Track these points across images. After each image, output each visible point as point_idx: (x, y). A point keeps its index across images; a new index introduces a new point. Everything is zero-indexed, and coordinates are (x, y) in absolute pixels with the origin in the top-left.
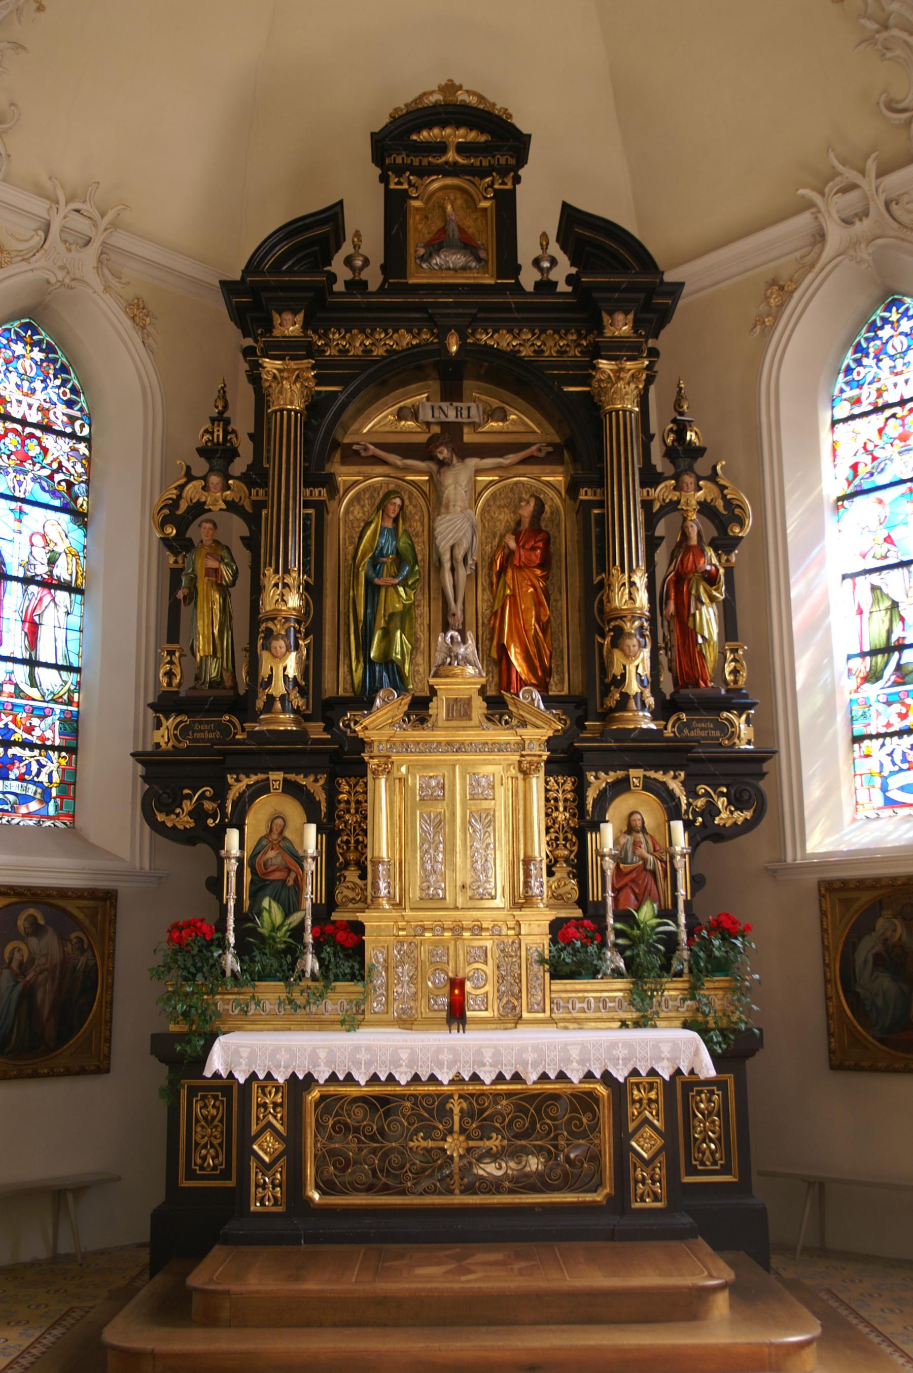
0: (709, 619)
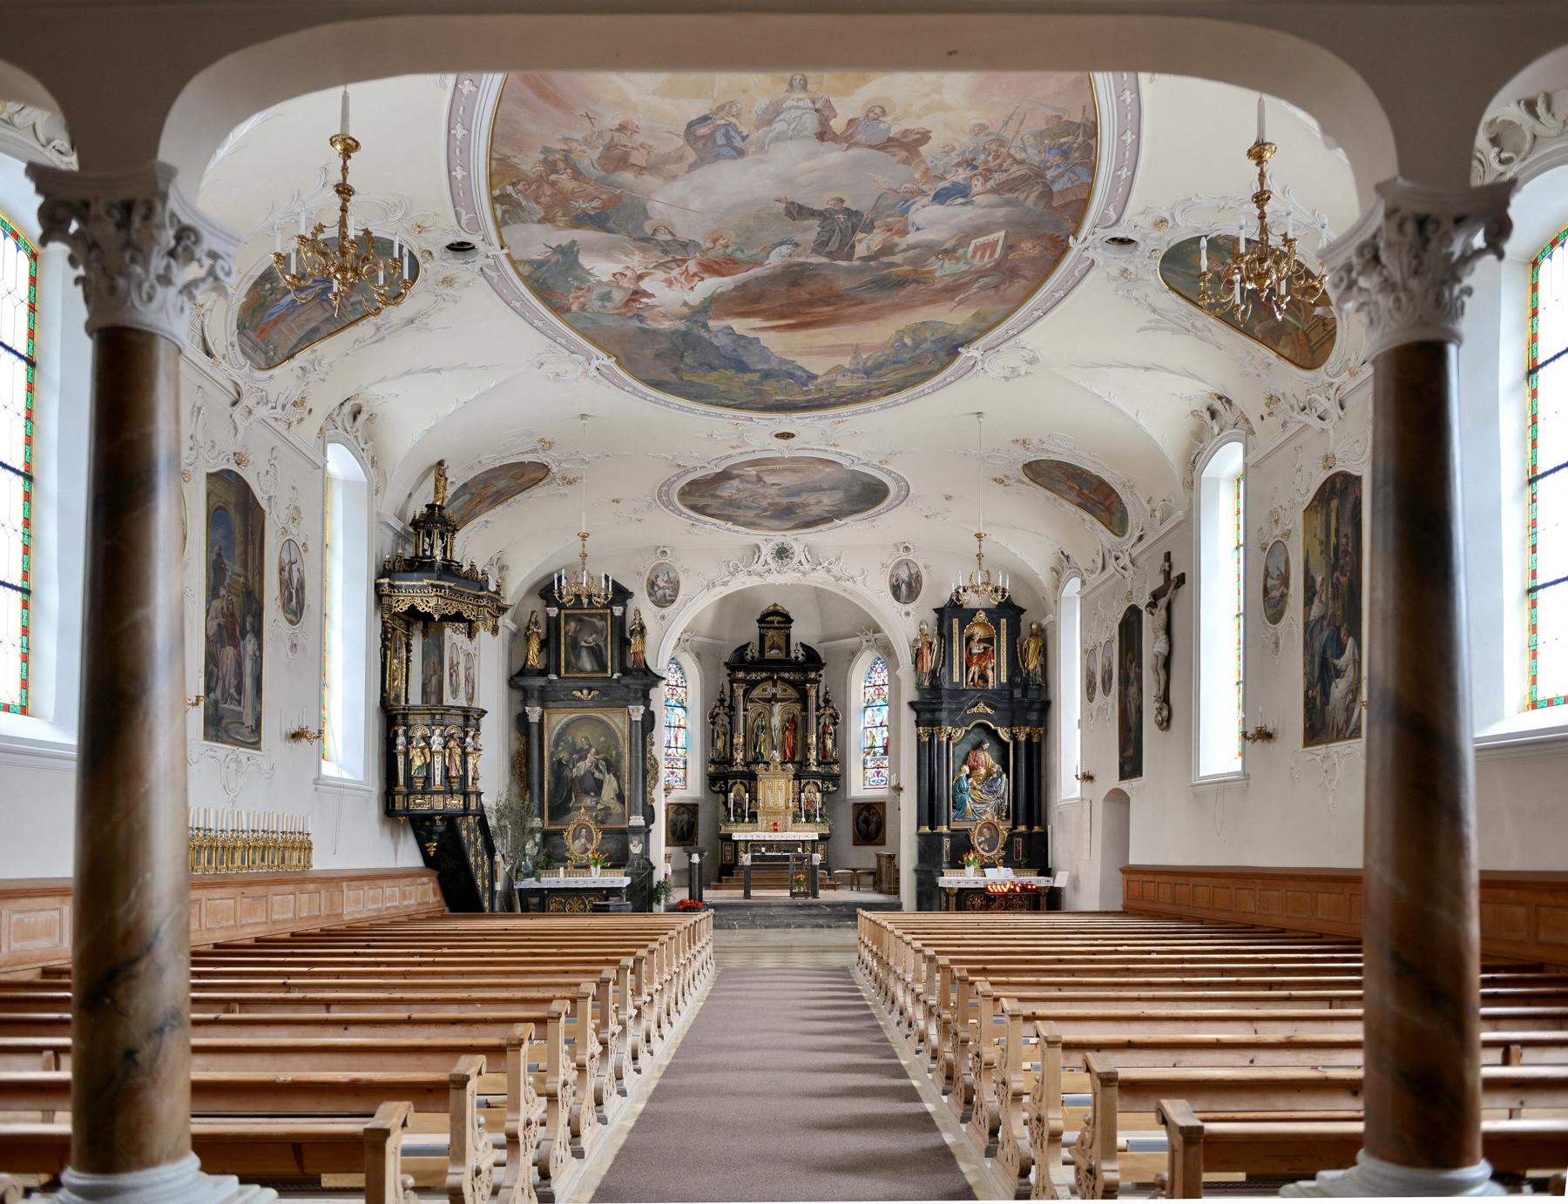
0: (829, 743)
